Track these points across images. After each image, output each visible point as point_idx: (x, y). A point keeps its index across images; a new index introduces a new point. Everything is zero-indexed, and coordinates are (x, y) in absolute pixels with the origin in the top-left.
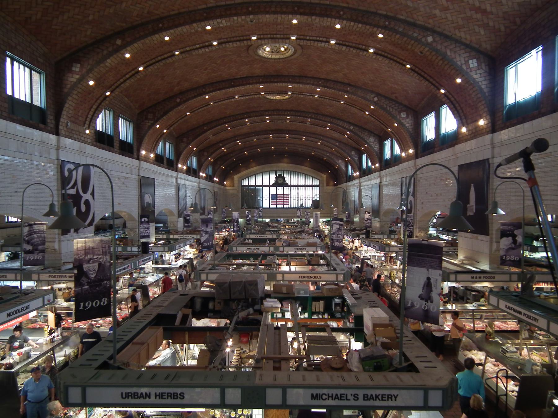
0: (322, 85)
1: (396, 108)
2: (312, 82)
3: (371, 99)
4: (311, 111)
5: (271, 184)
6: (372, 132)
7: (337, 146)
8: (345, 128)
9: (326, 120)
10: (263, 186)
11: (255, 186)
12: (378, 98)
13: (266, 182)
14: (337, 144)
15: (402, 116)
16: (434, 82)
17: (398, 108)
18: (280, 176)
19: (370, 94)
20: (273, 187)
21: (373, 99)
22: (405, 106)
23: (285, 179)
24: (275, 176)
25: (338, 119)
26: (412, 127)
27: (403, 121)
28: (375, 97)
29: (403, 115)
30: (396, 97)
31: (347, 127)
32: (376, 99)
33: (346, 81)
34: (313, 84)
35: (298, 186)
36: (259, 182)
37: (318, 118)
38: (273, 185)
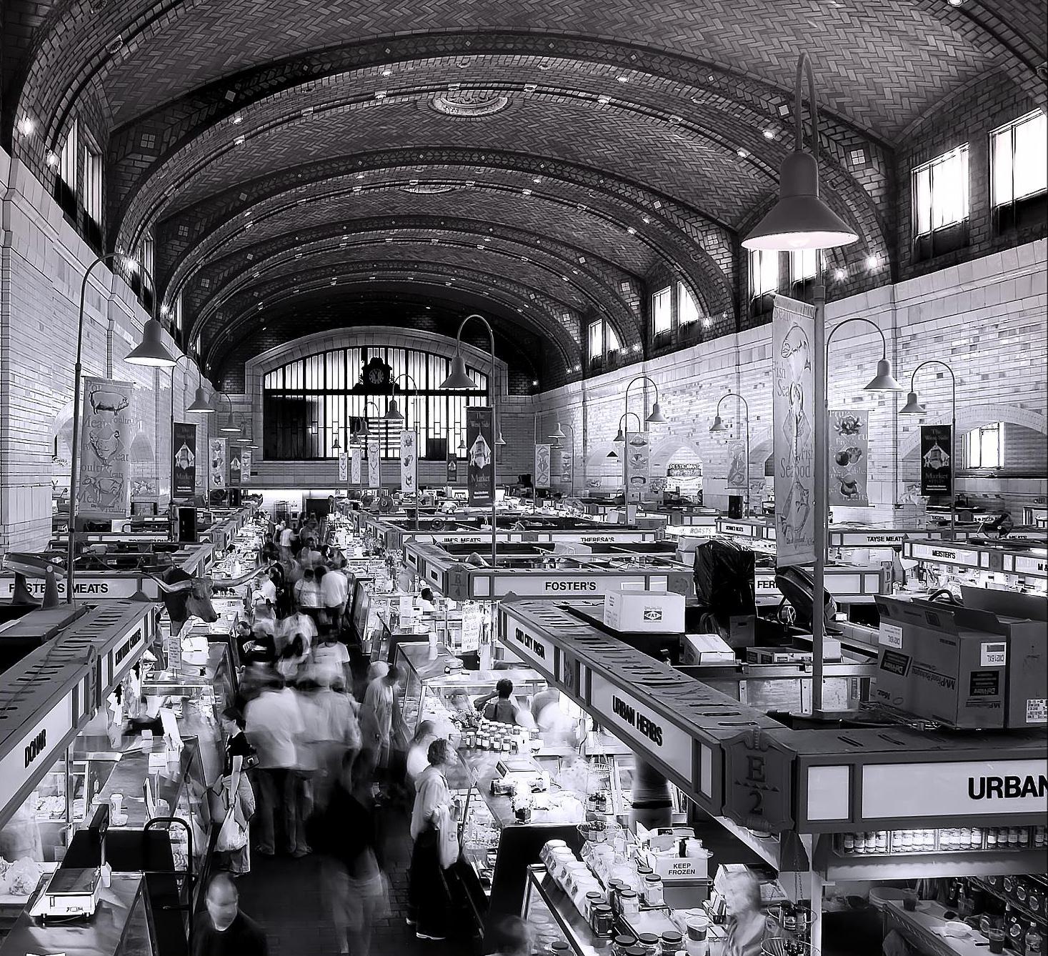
0: (639, 64)
1: (838, 137)
2: (610, 56)
3: (773, 111)
4: (547, 153)
5: (350, 387)
6: (714, 221)
7: (579, 266)
8: (639, 206)
9: (587, 180)
10: (325, 392)
11: (305, 392)
12: (790, 109)
13: (336, 382)
14: (582, 260)
15: (855, 162)
16: (1022, 48)
17: (844, 139)
18: (377, 362)
19: (767, 97)
20: (356, 397)
21: (778, 111)
22: (862, 133)
23: (391, 372)
24: (362, 365)
25: (620, 180)
26: (881, 192)
27: (858, 175)
28: (782, 104)
29: (858, 158)
30: (840, 105)
31: (645, 203)
32: (784, 111)
33: (706, 56)
34: (613, 62)
35: (427, 393)
36: (314, 383)
37: (566, 174)
38: (357, 390)
